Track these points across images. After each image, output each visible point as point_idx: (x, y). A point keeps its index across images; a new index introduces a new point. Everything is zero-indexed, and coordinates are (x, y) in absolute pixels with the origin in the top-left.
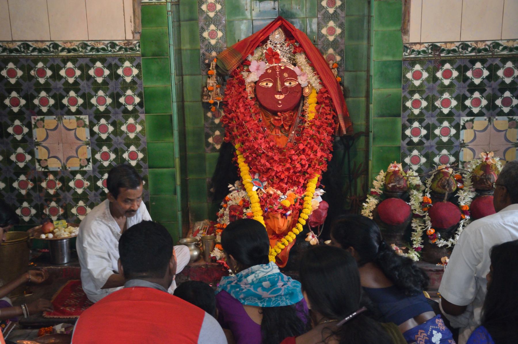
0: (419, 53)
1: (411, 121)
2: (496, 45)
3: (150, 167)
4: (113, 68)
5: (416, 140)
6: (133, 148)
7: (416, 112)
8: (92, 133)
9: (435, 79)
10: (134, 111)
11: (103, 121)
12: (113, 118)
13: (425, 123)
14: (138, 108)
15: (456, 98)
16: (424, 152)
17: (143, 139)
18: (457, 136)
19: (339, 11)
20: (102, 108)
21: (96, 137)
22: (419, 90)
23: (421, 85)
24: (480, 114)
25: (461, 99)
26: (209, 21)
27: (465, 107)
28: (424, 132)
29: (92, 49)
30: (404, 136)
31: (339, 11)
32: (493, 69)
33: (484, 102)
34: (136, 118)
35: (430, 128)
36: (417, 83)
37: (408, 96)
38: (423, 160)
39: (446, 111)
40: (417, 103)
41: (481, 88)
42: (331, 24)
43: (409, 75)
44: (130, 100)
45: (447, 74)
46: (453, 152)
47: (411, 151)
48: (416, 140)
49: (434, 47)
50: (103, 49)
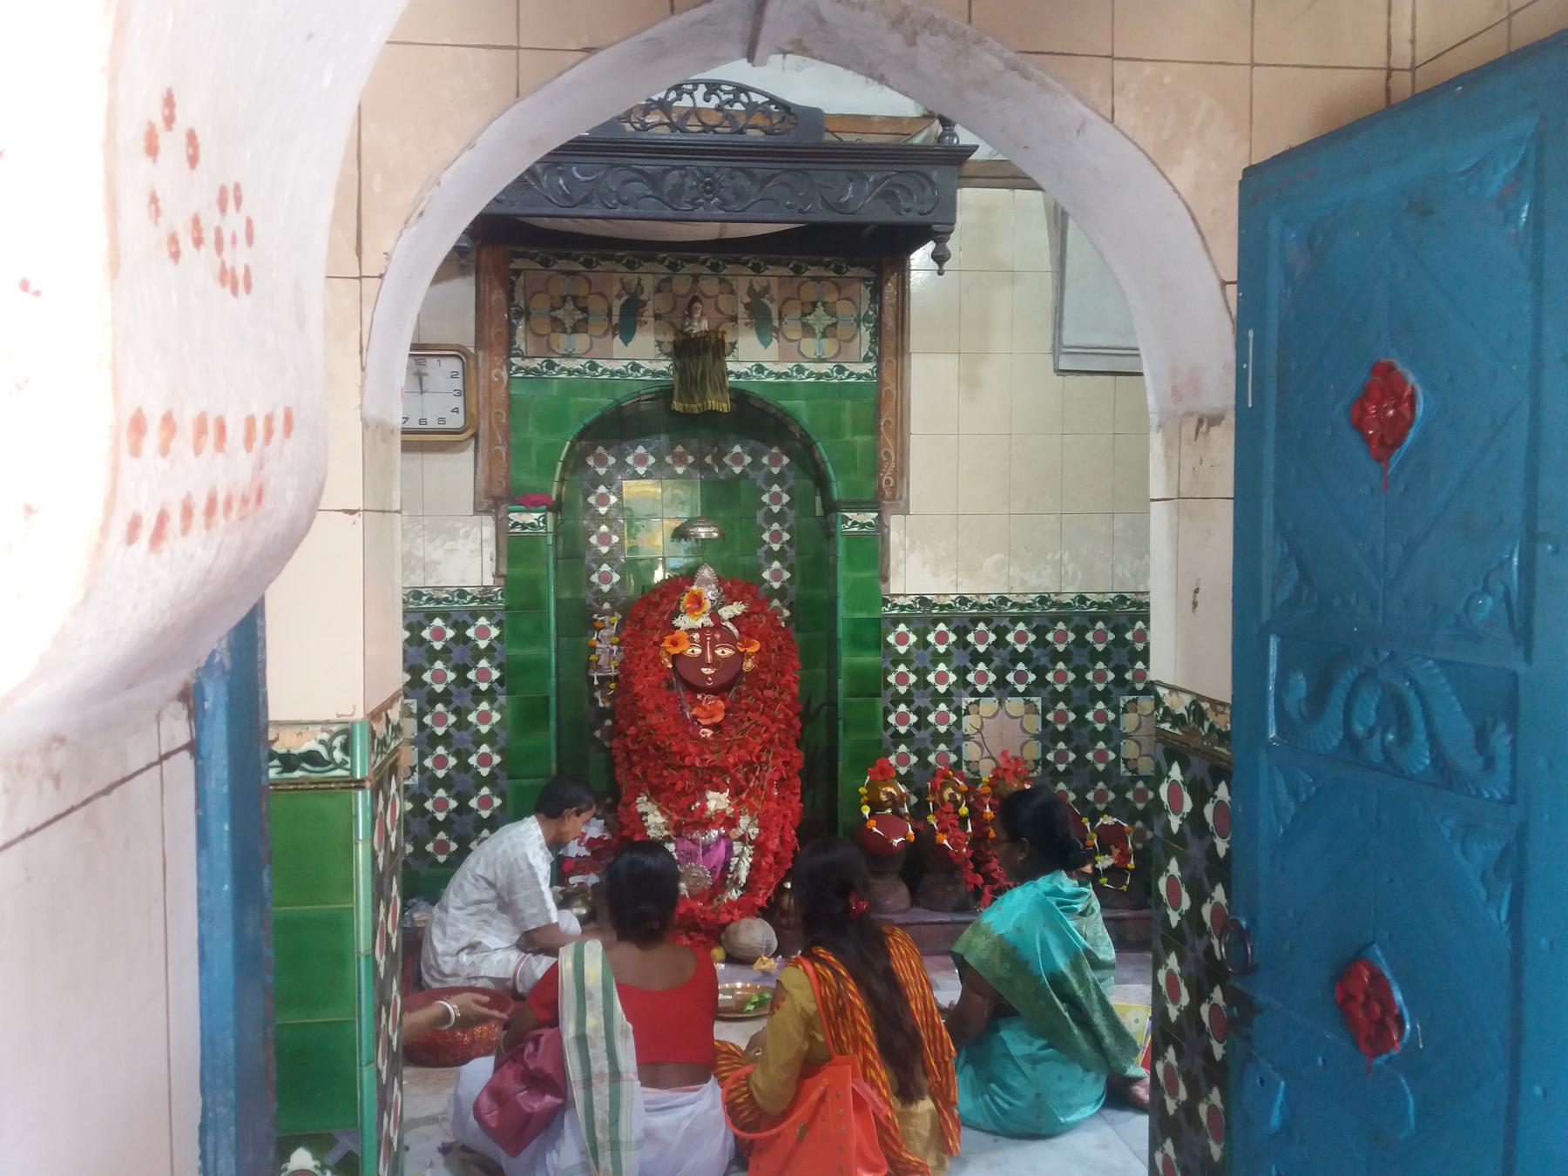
0: (902, 608)
1: (896, 704)
2: (1003, 600)
3: (510, 777)
4: (460, 626)
5: (903, 730)
6: (484, 748)
7: (903, 690)
8: (422, 727)
9: (927, 644)
10: (491, 690)
11: (440, 707)
12: (456, 702)
13: (914, 707)
14: (497, 687)
15: (955, 671)
16: (914, 748)
17: (503, 734)
18: (958, 724)
19: (787, 548)
20: (439, 688)
21: (427, 732)
22: (905, 659)
23: (908, 651)
24: (988, 694)
25: (962, 672)
26: (600, 560)
27: (967, 684)
28: (914, 719)
29: (430, 600)
30: (887, 725)
31: (787, 548)
32: (1001, 632)
33: (992, 677)
34: (492, 702)
35: (922, 713)
36: (902, 649)
37: (891, 667)
38: (914, 759)
39: (942, 689)
40: (902, 678)
41: (986, 658)
42: (776, 565)
43: (891, 639)
44: (484, 674)
45: (942, 638)
46: (954, 747)
47: (896, 746)
48: (903, 730)
49: (923, 600)
50: (446, 599)
